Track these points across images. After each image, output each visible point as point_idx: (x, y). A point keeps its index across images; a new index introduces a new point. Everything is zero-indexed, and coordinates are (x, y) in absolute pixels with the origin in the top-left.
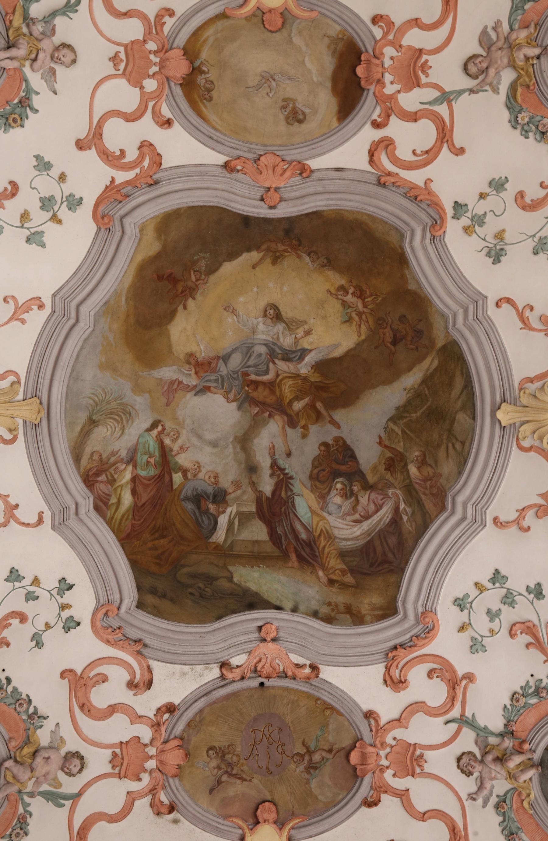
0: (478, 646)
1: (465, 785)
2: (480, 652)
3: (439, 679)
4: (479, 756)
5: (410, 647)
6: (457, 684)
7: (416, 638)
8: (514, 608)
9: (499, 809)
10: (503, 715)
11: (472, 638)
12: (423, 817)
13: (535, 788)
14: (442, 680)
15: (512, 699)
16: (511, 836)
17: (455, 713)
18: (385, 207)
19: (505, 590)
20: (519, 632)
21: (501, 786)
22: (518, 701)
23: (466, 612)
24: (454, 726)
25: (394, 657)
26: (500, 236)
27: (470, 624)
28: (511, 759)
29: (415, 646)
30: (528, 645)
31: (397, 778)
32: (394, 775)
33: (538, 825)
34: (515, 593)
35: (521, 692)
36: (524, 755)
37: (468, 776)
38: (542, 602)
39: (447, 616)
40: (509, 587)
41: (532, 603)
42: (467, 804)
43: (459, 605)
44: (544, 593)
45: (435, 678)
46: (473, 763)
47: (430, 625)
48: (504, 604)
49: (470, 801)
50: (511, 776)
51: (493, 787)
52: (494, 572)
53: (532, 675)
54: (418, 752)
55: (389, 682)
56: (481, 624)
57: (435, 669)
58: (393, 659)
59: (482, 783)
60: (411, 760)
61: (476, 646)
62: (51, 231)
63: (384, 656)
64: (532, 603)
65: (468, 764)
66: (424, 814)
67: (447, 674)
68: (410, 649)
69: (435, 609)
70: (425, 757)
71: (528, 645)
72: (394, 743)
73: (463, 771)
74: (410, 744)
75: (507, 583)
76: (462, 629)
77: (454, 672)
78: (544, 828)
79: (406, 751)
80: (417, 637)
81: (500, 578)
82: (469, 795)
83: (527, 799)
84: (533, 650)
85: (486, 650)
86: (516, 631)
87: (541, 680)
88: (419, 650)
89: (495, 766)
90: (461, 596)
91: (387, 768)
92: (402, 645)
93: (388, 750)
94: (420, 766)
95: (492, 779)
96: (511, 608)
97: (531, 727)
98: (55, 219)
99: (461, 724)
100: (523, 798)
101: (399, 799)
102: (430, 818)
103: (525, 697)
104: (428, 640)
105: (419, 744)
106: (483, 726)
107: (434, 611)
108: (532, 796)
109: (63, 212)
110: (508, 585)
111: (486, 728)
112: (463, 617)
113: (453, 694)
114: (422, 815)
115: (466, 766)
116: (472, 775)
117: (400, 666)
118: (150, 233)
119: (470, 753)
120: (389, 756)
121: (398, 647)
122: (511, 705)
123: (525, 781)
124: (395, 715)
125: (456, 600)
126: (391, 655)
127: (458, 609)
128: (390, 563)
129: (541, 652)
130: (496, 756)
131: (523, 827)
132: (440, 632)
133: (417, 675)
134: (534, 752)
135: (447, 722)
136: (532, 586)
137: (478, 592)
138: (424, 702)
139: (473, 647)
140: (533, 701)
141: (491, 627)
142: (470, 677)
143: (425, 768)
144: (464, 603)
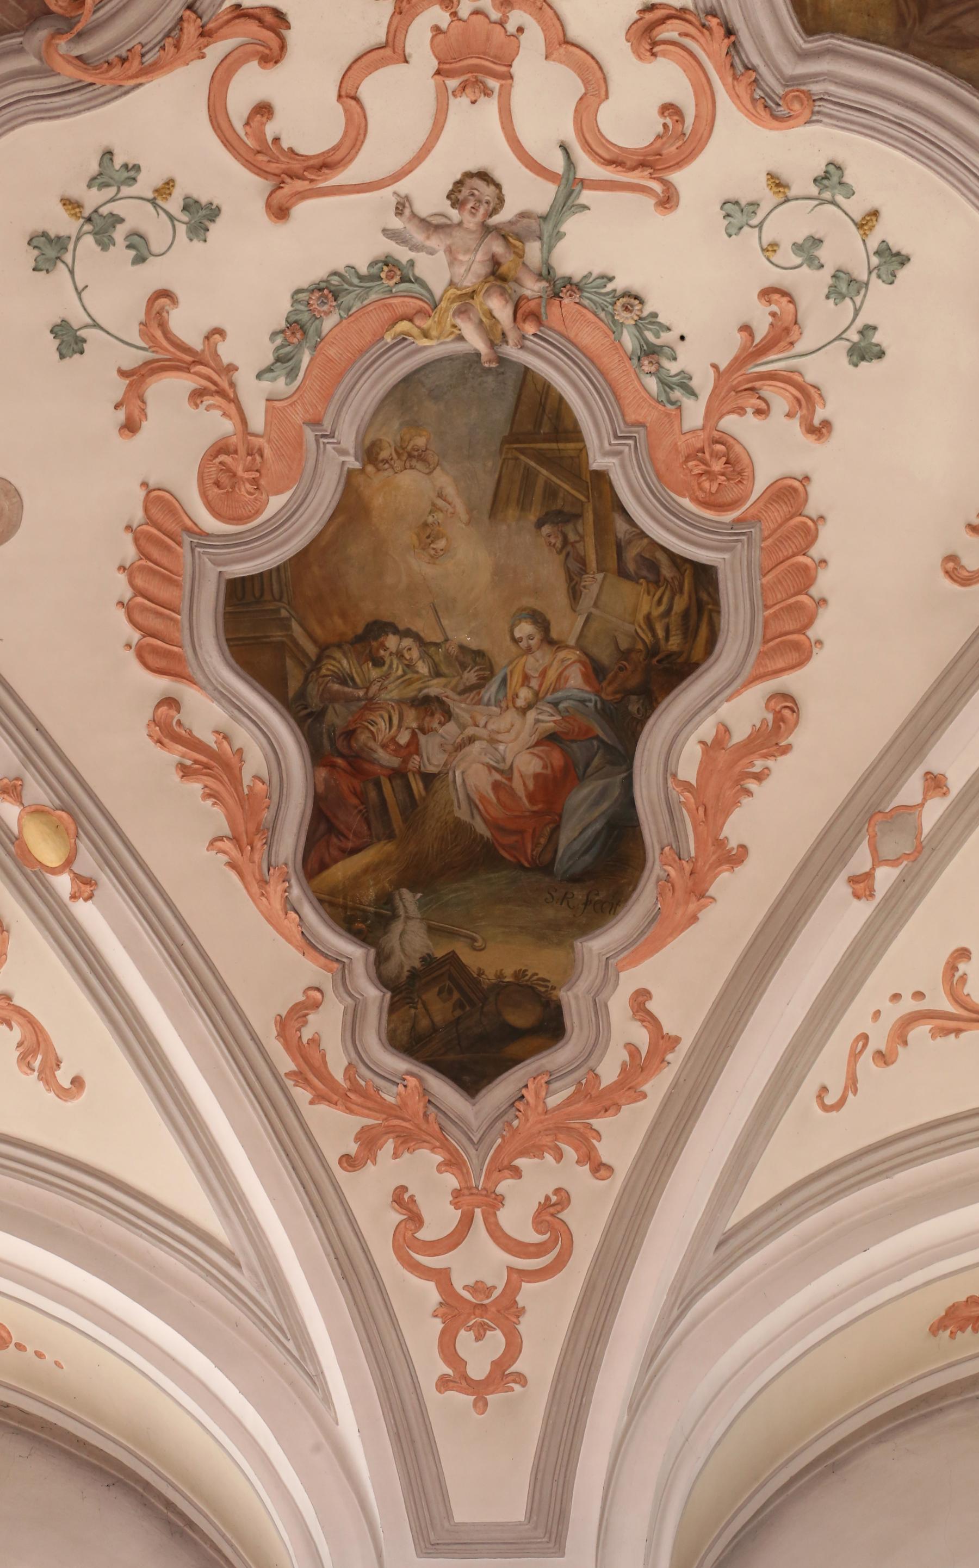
0: (738, 219)
1: (429, 190)
2: (726, 222)
3: (660, 129)
4: (496, 220)
5: (732, 65)
6: (654, 166)
7: (753, 78)
8: (828, 297)
9: (386, 269)
10: (590, 273)
11: (755, 205)
12: (348, 96)
13: (443, 347)
14: (659, 137)
15: (627, 294)
16: (330, 295)
17: (588, 168)
19: (864, 277)
20: (774, 308)
21: (434, 270)
22: (626, 308)
23: (814, 190)
24: (557, 163)
25: (709, 29)
27: (787, 200)
28: (507, 302)
29: (735, 77)
30: (746, 329)
31: (430, 35)
32: (437, 30)
33: (362, 352)
34: (858, 300)
35: (645, 314)
36: (512, 325)
37: (448, 197)
38: (844, 360)
39: (803, 148)
40: (870, 286)
41: (839, 338)
42: (387, 192)
43: (827, 176)
44: (863, 364)
45: (662, 121)
46: (482, 211)
47: (782, 111)
48: (834, 276)
49: (394, 201)
50: (465, 300)
51: (432, 252)
52: (904, 252)
53: (682, 338)
54: (493, 84)
55: (649, 17)
56: (789, 224)
57: (683, 122)
58: (704, 26)
59: (438, 228)
60: (474, 66)
61: (738, 214)
63: (709, 5)
64: (839, 338)
65: (480, 201)
66: (355, 98)
67: (674, 148)
68: (728, 67)
69: (821, 121)
70: (483, 99)
71: (746, 329)
72: (511, 27)
73: (459, 184)
74: (510, 66)
75: (880, 281)
76: (777, 183)
77: (680, 164)
78: (357, 366)
79: (495, 57)
80: (756, 81)
81: (892, 268)
82: (407, 197)
83: (415, 331)
84: (738, 339)
85: (730, 236)
86: (777, 303)
87: (675, 359)
88: (724, 85)
89: (483, 262)
90: (847, 179)
91: (454, 14)
92: (735, 46)
93: (495, 15)
94: (463, 87)
95: (449, 251)
96: (826, 291)
97: (572, 335)
99: (564, 181)
100: (417, 322)
101: (383, 38)
102: (346, 111)
103: (636, 325)
104: (750, 106)
105: (511, 85)
106: (563, 228)
107: (814, 118)
108: (425, 342)
110: (875, 283)
111: (560, 236)
112: (802, 184)
113: (629, 164)
114: (352, 94)
115: (473, 195)
116: (453, 206)
117: (687, 42)
119: (501, 200)
120: (480, 18)
121: (733, 38)
122: (615, 291)
123: (454, 326)
124: (575, 31)
125: (839, 168)
126: (713, 22)
127: (820, 172)
128: (921, 17)
129: (736, 359)
130: (502, 260)
131: (352, 319)
132: (766, 132)
133: (666, 80)
134: (522, 347)
135: (564, 147)
136: (877, 338)
137: (858, 218)
138: (607, 97)
139: (736, 207)
140: (628, 341)
141: (782, 246)
142: (668, 201)
143: (459, 99)
144: (834, 188)
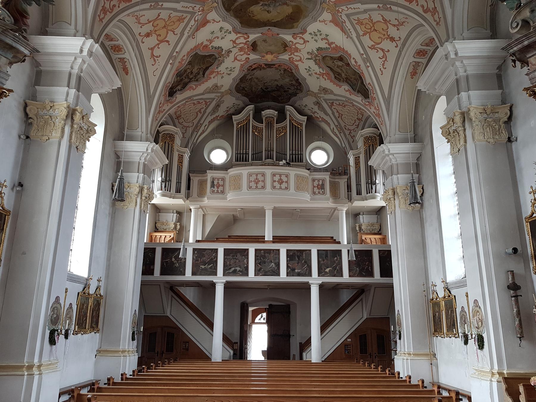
18: (245, 30)
26: (221, 31)
62: (316, 31)
98: (315, 33)
109: (313, 33)
118: (295, 26)
